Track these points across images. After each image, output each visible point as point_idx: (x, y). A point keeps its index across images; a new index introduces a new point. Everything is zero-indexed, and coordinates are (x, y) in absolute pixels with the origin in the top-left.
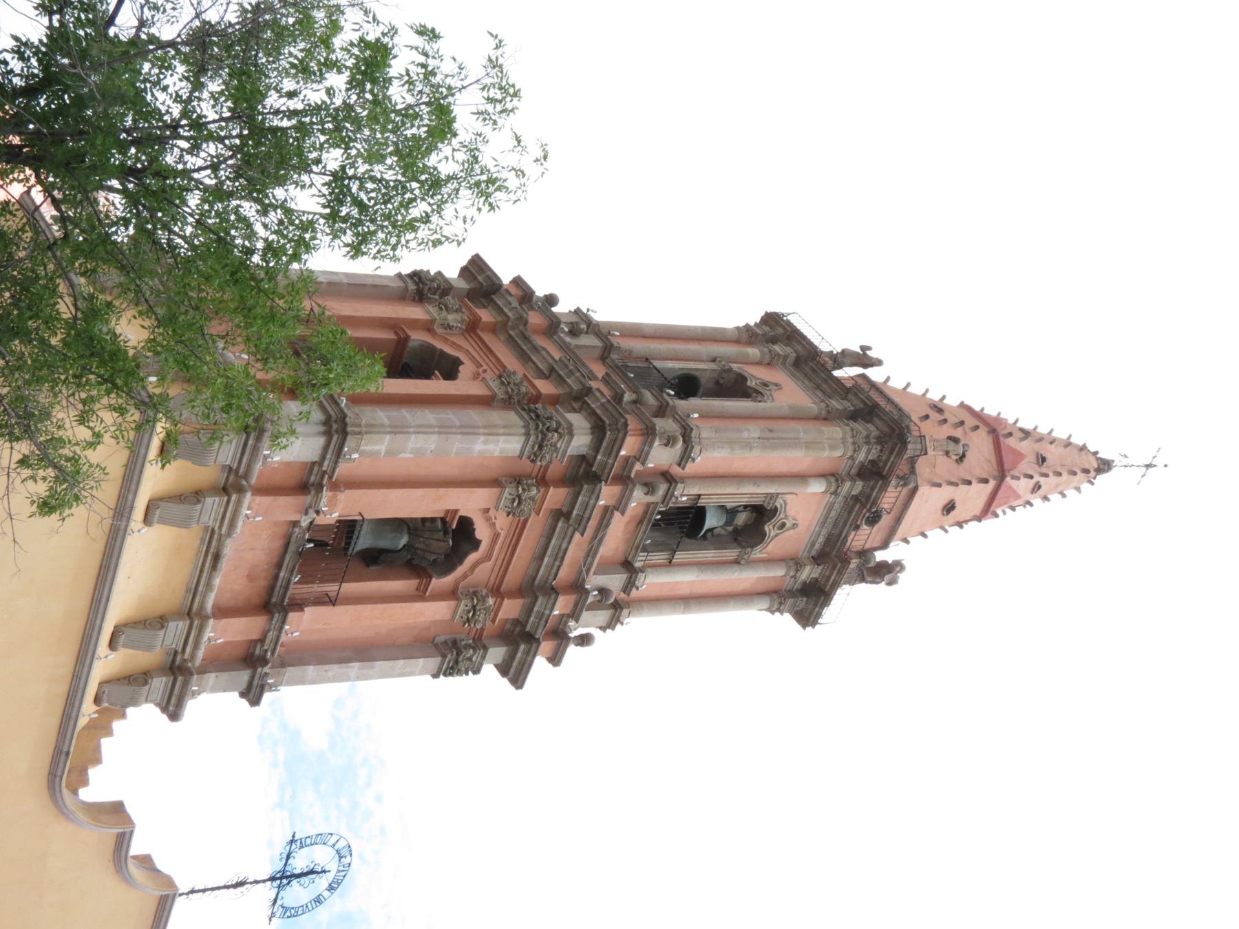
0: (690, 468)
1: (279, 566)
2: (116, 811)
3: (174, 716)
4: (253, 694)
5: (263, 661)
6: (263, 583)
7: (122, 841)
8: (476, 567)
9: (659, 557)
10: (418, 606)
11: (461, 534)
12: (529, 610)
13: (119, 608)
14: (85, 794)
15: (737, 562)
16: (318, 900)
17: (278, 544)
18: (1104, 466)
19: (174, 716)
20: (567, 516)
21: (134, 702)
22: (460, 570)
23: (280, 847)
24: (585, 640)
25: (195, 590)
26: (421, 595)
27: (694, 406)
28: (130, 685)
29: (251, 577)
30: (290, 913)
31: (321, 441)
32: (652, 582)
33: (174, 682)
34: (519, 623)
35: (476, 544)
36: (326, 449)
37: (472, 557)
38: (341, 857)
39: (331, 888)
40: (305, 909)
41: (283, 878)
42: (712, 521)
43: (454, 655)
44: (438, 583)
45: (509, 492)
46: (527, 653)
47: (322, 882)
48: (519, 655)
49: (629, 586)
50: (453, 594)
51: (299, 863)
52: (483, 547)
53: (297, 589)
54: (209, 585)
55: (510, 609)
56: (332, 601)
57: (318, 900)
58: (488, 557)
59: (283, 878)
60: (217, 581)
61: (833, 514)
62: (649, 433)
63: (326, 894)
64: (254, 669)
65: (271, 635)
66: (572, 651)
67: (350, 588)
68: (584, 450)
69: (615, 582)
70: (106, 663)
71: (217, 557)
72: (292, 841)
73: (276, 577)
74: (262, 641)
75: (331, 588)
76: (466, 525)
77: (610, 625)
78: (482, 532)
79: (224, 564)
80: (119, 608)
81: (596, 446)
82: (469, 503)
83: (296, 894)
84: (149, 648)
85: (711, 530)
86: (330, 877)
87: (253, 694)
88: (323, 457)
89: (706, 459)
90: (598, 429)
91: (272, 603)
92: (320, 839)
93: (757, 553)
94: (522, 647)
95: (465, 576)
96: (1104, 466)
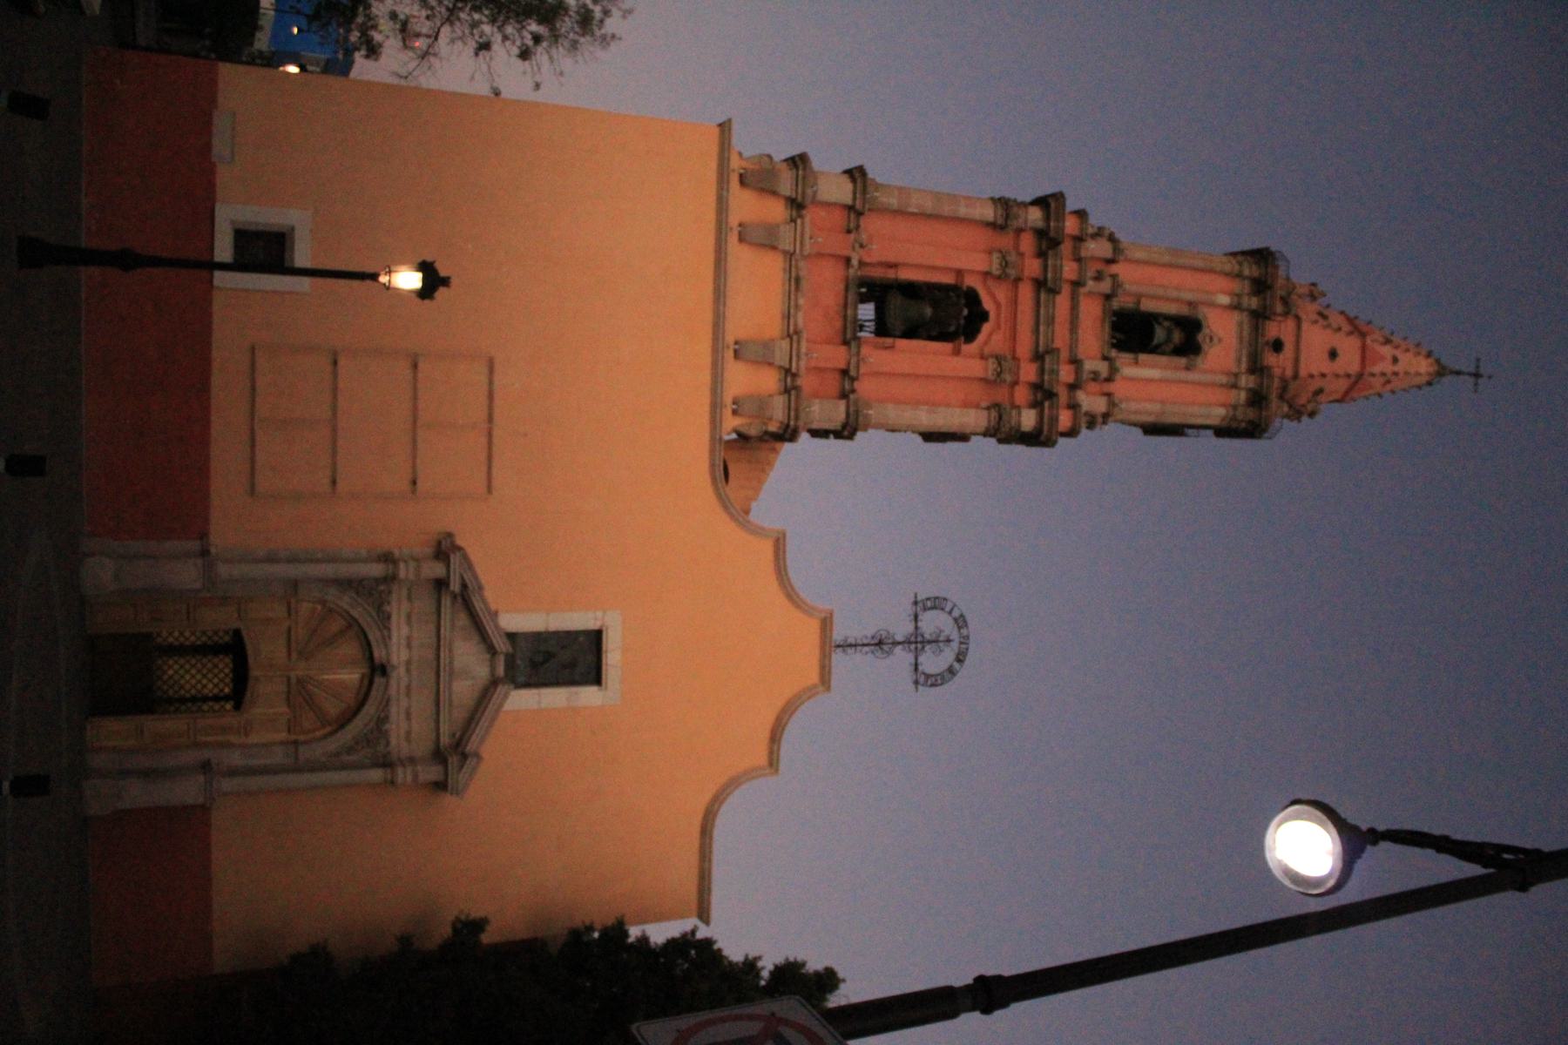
1: (845, 305)
6: (838, 324)
12: (1042, 371)
15: (1187, 368)
16: (951, 671)
17: (842, 286)
22: (981, 337)
26: (957, 352)
30: (934, 681)
35: (984, 317)
36: (855, 193)
37: (986, 328)
38: (959, 628)
41: (917, 642)
42: (1160, 334)
44: (967, 348)
46: (1051, 407)
48: (1046, 411)
52: (992, 315)
61: (1245, 333)
63: (957, 666)
65: (854, 361)
72: (916, 603)
73: (845, 317)
76: (972, 298)
78: (987, 304)
81: (1047, 218)
83: (932, 662)
85: (1158, 346)
88: (854, 199)
94: (1047, 404)
95: (986, 343)
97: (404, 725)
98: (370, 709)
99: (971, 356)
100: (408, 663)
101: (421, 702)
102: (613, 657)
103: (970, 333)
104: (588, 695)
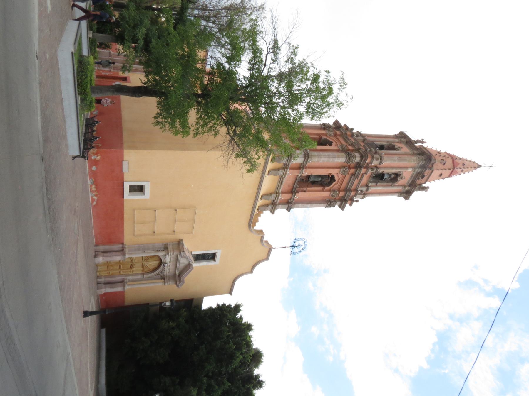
0: (382, 165)
1: (294, 184)
2: (261, 232)
3: (273, 213)
4: (289, 209)
5: (291, 203)
6: (291, 187)
7: (262, 237)
8: (335, 185)
9: (374, 184)
10: (323, 193)
11: (332, 178)
13: (263, 191)
14: (255, 228)
15: (391, 186)
16: (300, 251)
17: (294, 180)
18: (479, 166)
19: (273, 213)
20: (354, 175)
21: (265, 210)
23: (293, 240)
24: (357, 201)
25: (278, 188)
26: (323, 191)
27: (383, 152)
28: (264, 207)
29: (288, 186)
30: (295, 253)
31: (303, 159)
32: (372, 189)
33: (273, 206)
34: (343, 197)
35: (335, 180)
39: (303, 249)
40: (298, 253)
41: (293, 246)
42: (386, 177)
43: (330, 203)
44: (327, 188)
45: (342, 170)
47: (301, 248)
49: (367, 190)
50: (330, 191)
51: (296, 244)
53: (298, 189)
54: (280, 187)
55: (342, 194)
56: (305, 191)
57: (300, 251)
58: (337, 183)
59: (293, 246)
60: (282, 187)
62: (373, 158)
64: (289, 205)
66: (354, 203)
67: (309, 189)
68: (358, 161)
69: (364, 189)
70: (260, 202)
71: (282, 182)
74: (291, 199)
75: (305, 189)
76: (333, 176)
77: (363, 198)
78: (336, 178)
79: (283, 183)
80: (263, 191)
82: (333, 172)
83: (296, 250)
84: (268, 200)
86: (303, 247)
87: (289, 209)
89: (384, 164)
90: (362, 157)
91: (293, 191)
92: (301, 239)
93: (396, 184)
96: (479, 166)
97: (168, 271)
98: (160, 269)
99: (327, 191)
100: (170, 262)
101: (172, 268)
102: (218, 257)
103: (330, 183)
104: (211, 263)
